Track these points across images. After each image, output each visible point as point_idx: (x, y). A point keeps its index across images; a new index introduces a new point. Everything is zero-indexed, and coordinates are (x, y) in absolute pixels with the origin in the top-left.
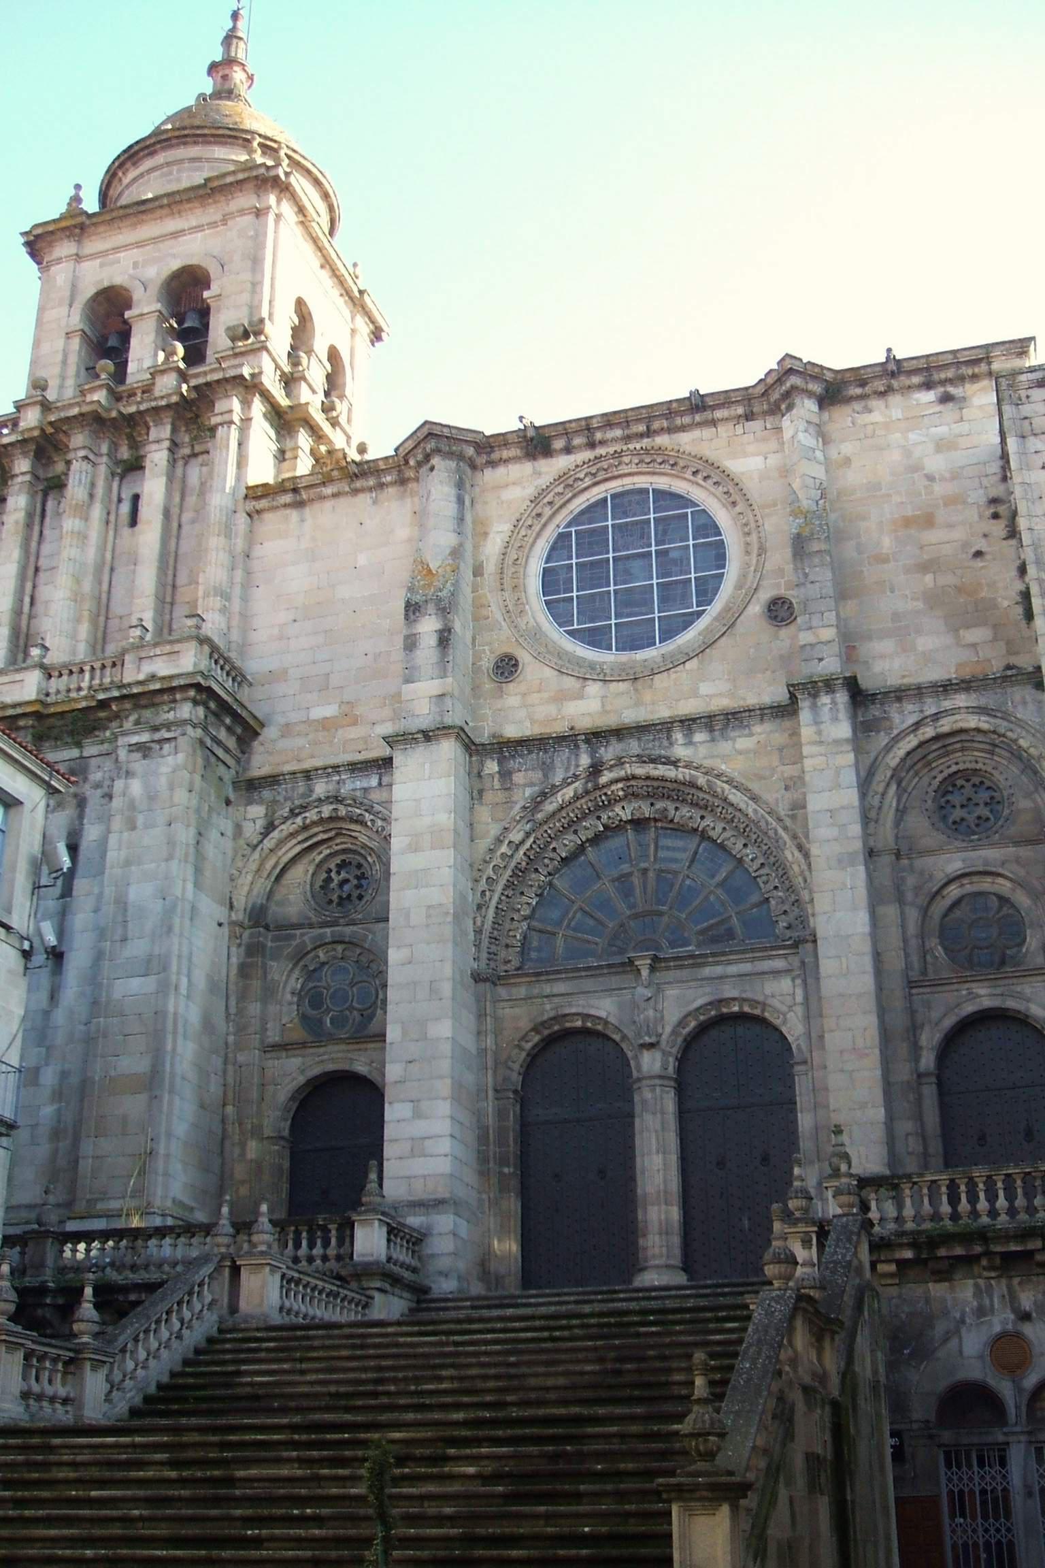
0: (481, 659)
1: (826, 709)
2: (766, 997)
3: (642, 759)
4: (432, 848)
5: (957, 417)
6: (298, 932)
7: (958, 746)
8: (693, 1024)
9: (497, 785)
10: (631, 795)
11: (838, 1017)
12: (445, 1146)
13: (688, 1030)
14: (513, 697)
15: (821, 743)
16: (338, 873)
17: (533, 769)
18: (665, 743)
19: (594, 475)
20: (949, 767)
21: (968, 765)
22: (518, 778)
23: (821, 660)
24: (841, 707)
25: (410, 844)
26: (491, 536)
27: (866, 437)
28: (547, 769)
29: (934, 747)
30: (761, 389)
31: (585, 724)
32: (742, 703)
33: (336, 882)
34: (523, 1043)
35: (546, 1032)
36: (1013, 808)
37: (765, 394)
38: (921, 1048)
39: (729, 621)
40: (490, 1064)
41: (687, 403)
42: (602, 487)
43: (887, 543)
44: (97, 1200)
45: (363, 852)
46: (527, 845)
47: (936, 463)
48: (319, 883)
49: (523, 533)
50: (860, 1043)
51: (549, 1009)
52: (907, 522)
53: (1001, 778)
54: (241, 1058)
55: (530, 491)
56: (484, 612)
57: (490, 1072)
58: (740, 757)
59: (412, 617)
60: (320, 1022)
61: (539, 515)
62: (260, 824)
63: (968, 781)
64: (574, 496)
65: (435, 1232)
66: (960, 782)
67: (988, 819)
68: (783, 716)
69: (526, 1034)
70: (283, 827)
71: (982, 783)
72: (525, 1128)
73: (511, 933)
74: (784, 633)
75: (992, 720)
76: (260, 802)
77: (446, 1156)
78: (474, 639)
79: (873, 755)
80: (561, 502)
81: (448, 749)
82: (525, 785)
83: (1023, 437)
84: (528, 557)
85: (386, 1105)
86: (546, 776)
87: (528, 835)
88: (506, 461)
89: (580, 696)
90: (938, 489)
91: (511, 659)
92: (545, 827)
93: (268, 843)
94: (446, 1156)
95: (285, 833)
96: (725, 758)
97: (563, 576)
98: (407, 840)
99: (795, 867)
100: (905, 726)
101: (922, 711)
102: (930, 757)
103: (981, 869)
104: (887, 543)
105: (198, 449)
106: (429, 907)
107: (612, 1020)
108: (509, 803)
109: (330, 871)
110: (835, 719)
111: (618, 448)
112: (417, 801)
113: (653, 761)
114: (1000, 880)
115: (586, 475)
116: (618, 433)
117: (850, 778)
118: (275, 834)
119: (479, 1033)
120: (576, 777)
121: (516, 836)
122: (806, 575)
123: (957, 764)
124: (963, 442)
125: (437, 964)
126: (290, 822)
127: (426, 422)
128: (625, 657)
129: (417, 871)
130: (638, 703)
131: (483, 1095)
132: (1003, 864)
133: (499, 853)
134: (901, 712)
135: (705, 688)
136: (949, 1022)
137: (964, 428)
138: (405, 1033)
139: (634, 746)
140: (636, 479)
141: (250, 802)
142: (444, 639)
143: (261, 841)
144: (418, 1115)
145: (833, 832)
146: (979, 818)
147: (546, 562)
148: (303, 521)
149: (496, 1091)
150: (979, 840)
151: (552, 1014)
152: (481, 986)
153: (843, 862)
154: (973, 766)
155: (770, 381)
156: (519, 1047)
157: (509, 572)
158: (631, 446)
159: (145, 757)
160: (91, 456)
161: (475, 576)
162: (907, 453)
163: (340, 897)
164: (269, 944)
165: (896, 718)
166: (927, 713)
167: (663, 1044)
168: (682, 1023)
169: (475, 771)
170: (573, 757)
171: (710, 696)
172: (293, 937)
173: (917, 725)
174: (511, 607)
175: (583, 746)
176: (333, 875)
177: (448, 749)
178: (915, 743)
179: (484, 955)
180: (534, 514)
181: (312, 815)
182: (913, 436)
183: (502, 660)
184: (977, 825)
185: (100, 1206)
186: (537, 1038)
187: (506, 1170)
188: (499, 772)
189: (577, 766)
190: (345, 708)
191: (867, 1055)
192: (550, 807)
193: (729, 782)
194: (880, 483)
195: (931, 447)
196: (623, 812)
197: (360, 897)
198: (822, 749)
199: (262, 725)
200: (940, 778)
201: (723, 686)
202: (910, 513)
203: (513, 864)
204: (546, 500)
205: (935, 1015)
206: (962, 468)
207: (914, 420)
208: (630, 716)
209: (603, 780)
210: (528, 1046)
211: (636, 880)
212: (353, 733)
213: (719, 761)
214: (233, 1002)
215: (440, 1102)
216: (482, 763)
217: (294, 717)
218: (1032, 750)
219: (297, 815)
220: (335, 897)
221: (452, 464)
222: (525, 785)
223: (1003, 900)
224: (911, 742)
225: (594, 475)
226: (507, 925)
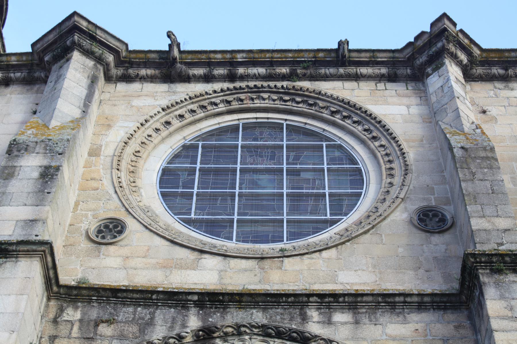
27: (509, 105)
37: (411, 59)
41: (333, 55)
42: (235, 116)
49: (150, 132)
55: (165, 102)
59: (16, 153)
61: (168, 123)
64: (206, 118)
68: (445, 309)
74: (436, 239)
78: (77, 204)
80: (192, 119)
84: (149, 155)
88: (143, 79)
89: (194, 266)
91: (116, 227)
97: (183, 177)
111: (259, 84)
115: (222, 101)
116: (262, 71)
122: (474, 174)
127: (75, 14)
140: (270, 115)
147: (168, 163)
155: (420, 43)
158: (272, 84)
161: (90, 154)
169: (52, 316)
174: (124, 184)
175: (193, 311)
180: (163, 120)
183: (106, 227)
188: (81, 321)
189: (184, 326)
216: (61, 310)
221: (91, 63)
225: (229, 102)
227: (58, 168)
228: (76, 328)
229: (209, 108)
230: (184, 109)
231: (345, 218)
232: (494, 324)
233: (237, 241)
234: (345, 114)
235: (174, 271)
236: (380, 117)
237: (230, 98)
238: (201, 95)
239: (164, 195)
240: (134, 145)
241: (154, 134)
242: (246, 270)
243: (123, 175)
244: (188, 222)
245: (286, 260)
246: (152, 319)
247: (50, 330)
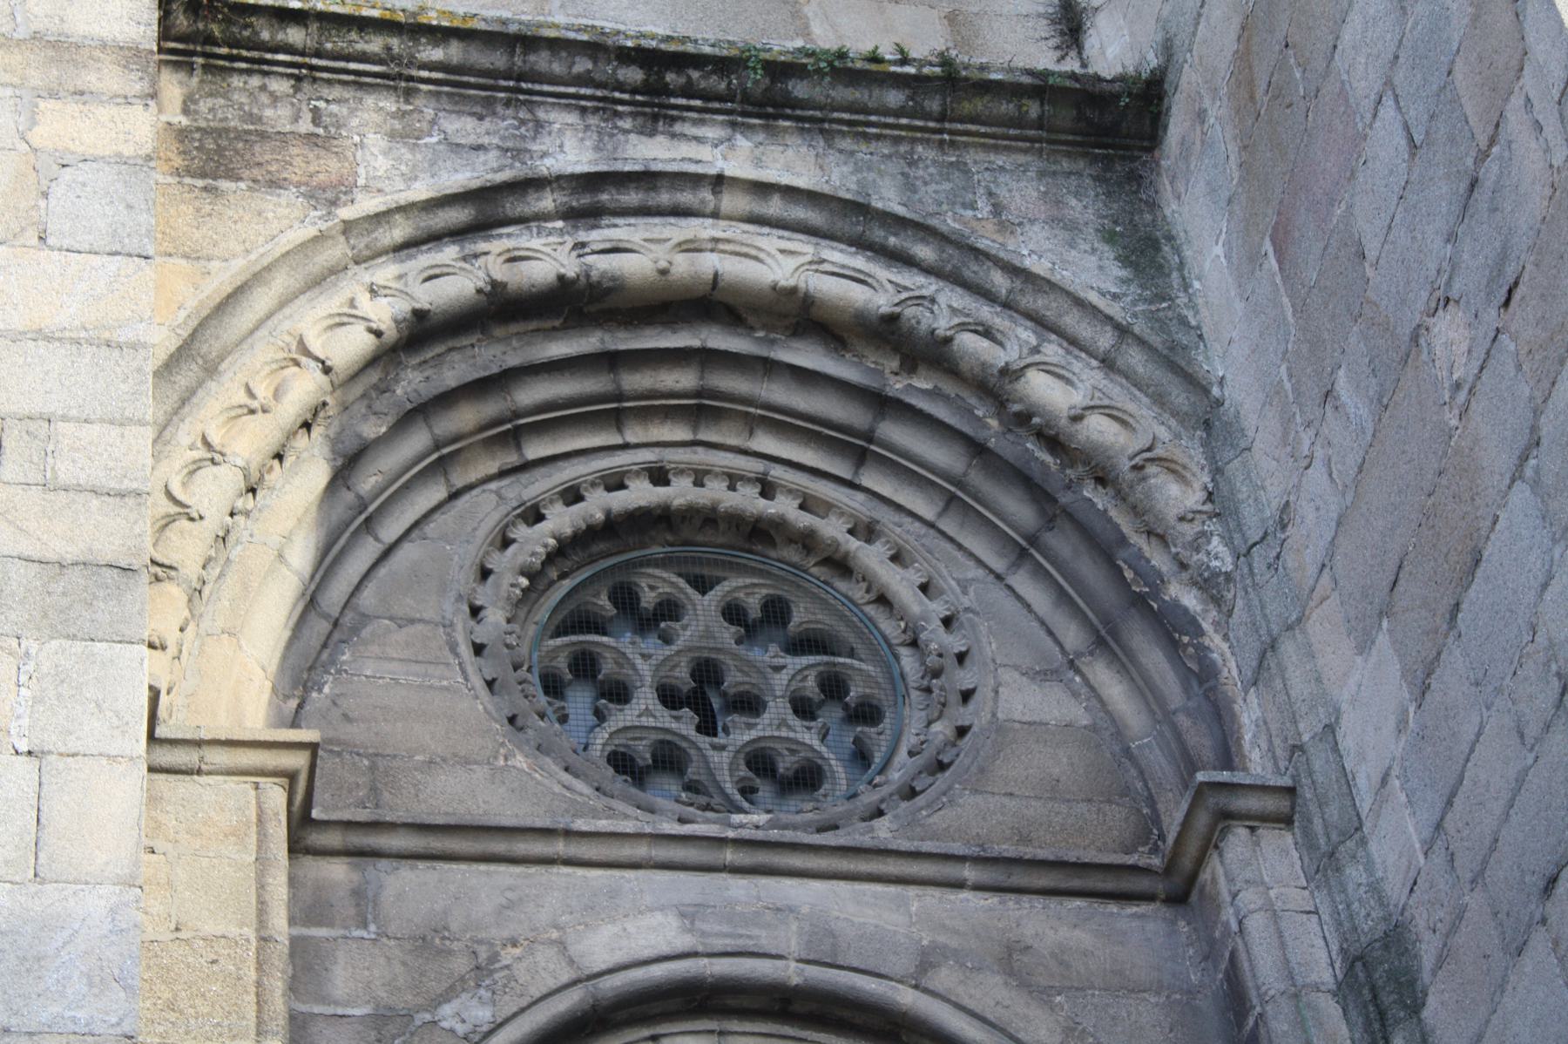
7: (682, 379)
20: (615, 482)
21: (715, 493)
29: (559, 348)
36: (964, 715)
53: (902, 584)
66: (653, 587)
67: (807, 779)
71: (776, 611)
75: (882, 272)
79: (221, 279)
101: (518, 153)
102: (531, 394)
103: (792, 973)
123: (659, 476)
132: (927, 961)
146: (760, 762)
154: (747, 500)
184: (748, 791)
200: (561, 520)
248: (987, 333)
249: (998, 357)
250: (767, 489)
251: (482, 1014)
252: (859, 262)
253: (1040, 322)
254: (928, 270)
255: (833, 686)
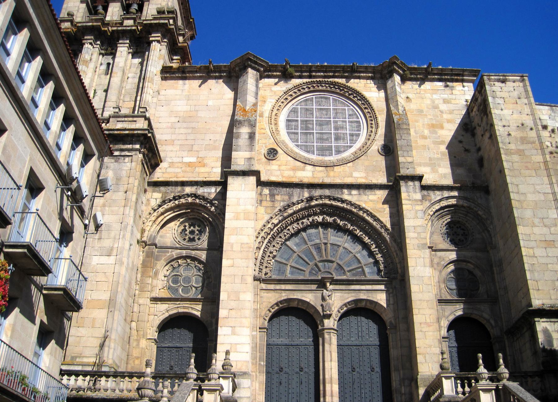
0: (261, 149)
1: (411, 187)
2: (378, 300)
3: (329, 198)
4: (245, 219)
5: (451, 93)
6: (170, 250)
8: (345, 308)
9: (268, 199)
10: (322, 213)
11: (419, 309)
12: (248, 348)
13: (343, 311)
14: (274, 165)
15: (410, 200)
16: (190, 227)
17: (284, 195)
18: (340, 193)
19: (309, 88)
22: (278, 198)
23: (408, 169)
24: (417, 187)
25: (234, 216)
26: (267, 103)
27: (417, 93)
28: (290, 196)
30: (380, 68)
31: (306, 181)
32: (370, 182)
33: (188, 231)
34: (271, 309)
35: (281, 306)
38: (442, 327)
39: (364, 150)
40: (258, 316)
43: (426, 132)
44: (76, 357)
45: (202, 220)
46: (279, 226)
47: (443, 107)
48: (180, 230)
49: (280, 104)
50: (428, 321)
51: (284, 296)
52: (433, 126)
54: (141, 301)
56: (263, 131)
57: (258, 319)
58: (370, 202)
59: (238, 126)
60: (177, 290)
62: (159, 201)
63: (455, 225)
65: (242, 386)
67: (463, 241)
69: (273, 306)
70: (169, 204)
71: (460, 227)
72: (269, 346)
73: (269, 262)
76: (160, 192)
77: (247, 353)
81: (252, 180)
82: (281, 201)
83: (494, 98)
85: (219, 328)
86: (290, 198)
87: (280, 222)
89: (303, 170)
90: (445, 116)
91: (274, 152)
92: (287, 220)
93: (161, 210)
94: (247, 353)
95: (169, 206)
96: (365, 202)
98: (233, 215)
99: (393, 249)
100: (436, 199)
101: (442, 195)
104: (426, 132)
105: (139, 50)
106: (242, 244)
107: (312, 303)
108: (273, 207)
109: (185, 226)
110: (415, 192)
111: (321, 80)
112: (239, 199)
113: (335, 199)
114: (469, 264)
115: (307, 87)
117: (420, 214)
118: (165, 206)
119: (254, 302)
120: (302, 201)
121: (275, 221)
122: (401, 137)
124: (453, 101)
125: (245, 268)
126: (173, 202)
128: (320, 158)
129: (237, 228)
130: (328, 176)
131: (255, 329)
133: (267, 227)
134: (435, 194)
135: (356, 174)
136: (452, 318)
137: (454, 97)
138: (228, 297)
139: (327, 192)
141: (154, 192)
142: (252, 136)
143: (158, 209)
144: (234, 333)
145: (415, 235)
148: (184, 84)
149: (260, 328)
150: (461, 248)
151: (285, 298)
152: (256, 282)
153: (422, 246)
154: (458, 219)
156: (269, 311)
157: (273, 117)
158: (326, 80)
159: (116, 161)
160: (93, 43)
162: (433, 101)
163: (189, 238)
164: (156, 253)
165: (433, 197)
166: (445, 196)
167: (334, 315)
168: (341, 308)
169: (259, 192)
170: (301, 192)
171: (358, 178)
172: (168, 252)
173: (440, 200)
176: (187, 228)
177: (252, 180)
178: (439, 207)
179: (257, 269)
180: (284, 98)
181: (183, 201)
182: (435, 96)
185: (78, 360)
186: (277, 308)
187: (262, 363)
188: (269, 194)
189: (303, 196)
190: (200, 160)
191: (431, 326)
192: (290, 211)
193: (366, 211)
194: (423, 110)
195: (441, 101)
196: (320, 219)
197: (199, 239)
198: (410, 202)
199: (161, 162)
201: (363, 174)
202: (434, 123)
203: (272, 233)
204: (290, 94)
205: (447, 314)
206: (453, 110)
207: (435, 91)
208: (328, 181)
209: (314, 203)
210: (273, 311)
211: (323, 247)
212: (202, 170)
213: (362, 202)
214: (139, 276)
215: (245, 329)
216: (262, 190)
217: (176, 160)
218: (484, 216)
219: (176, 200)
220: (187, 237)
222: (281, 201)
223: (470, 272)
224: (437, 207)
226: (266, 258)
227: (254, 134)
228: (268, 196)
229: (302, 90)
230: (292, 92)
231: (354, 145)
232: (404, 202)
233: (317, 155)
234: (355, 95)
235: (297, 172)
236: (368, 99)
237: (310, 86)
238: (299, 85)
239: (288, 133)
240: (275, 111)
241: (282, 105)
242: (321, 171)
243: (273, 126)
244: (297, 146)
245: (335, 167)
246: (292, 193)
247: (260, 198)
248: (475, 207)
249: (477, 210)
250: (460, 218)
251: (444, 263)
252: (466, 202)
253: (479, 207)
254: (472, 202)
255: (464, 233)
